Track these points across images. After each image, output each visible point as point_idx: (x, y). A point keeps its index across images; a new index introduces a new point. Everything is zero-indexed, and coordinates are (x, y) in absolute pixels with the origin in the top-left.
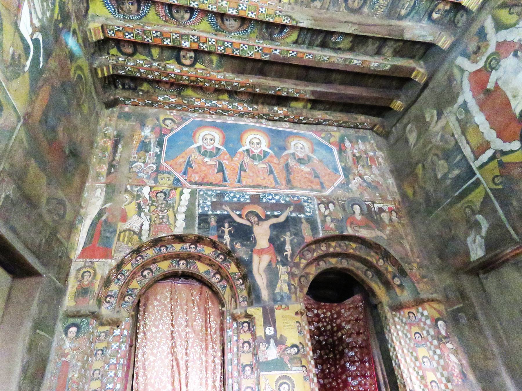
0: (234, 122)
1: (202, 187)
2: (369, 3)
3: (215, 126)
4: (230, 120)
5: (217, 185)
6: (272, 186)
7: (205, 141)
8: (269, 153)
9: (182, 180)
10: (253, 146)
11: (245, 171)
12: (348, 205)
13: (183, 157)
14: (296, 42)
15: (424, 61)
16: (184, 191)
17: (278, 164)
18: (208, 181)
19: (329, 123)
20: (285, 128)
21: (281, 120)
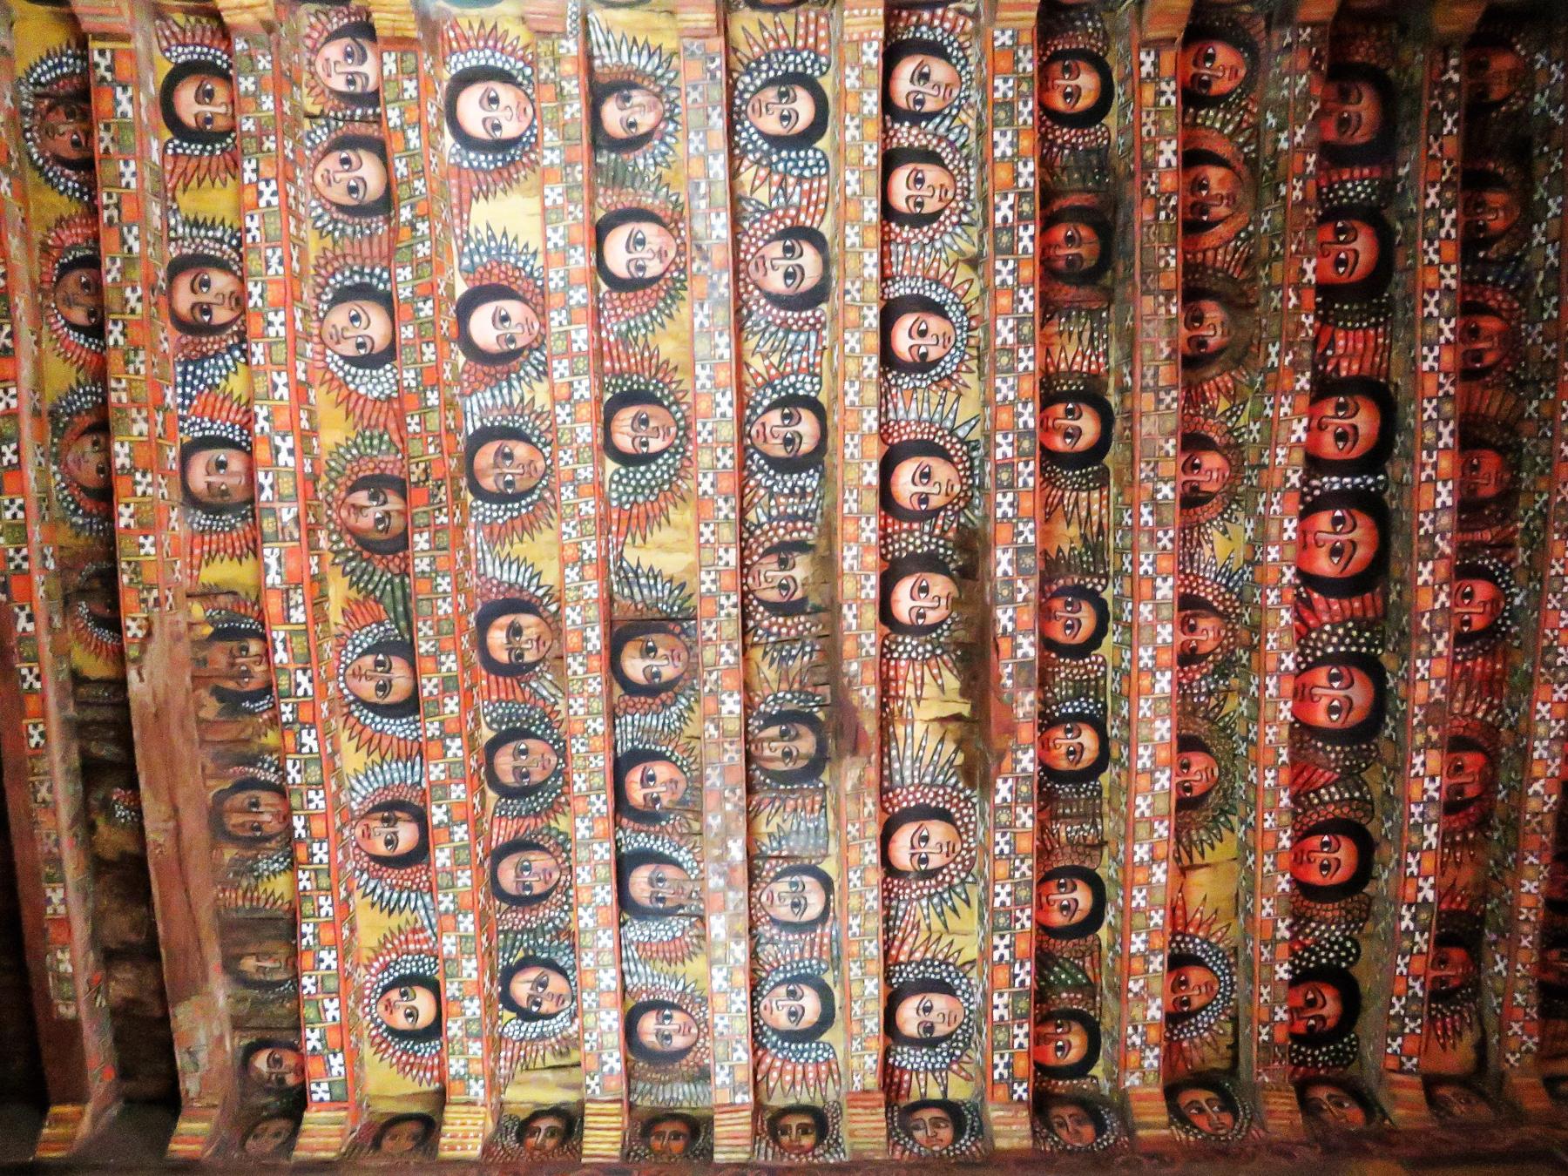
2: (250, 853)
14: (77, 678)
15: (121, 1114)
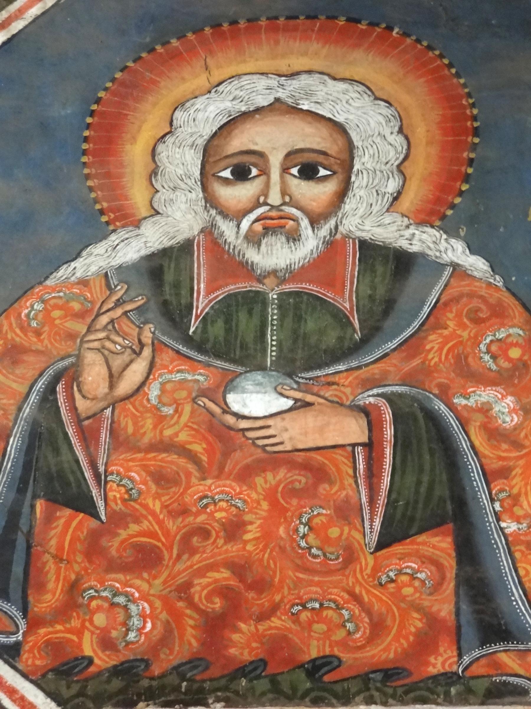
18: (279, 643)
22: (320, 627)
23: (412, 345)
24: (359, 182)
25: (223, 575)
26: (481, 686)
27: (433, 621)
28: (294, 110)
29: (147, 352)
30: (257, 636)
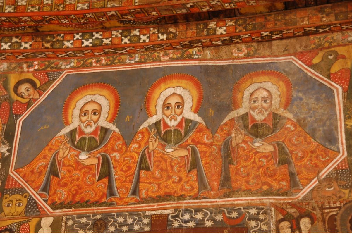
0: (138, 67)
1: (71, 211)
3: (101, 81)
4: (131, 63)
5: (97, 203)
6: (192, 194)
7: (84, 118)
8: (196, 123)
9: (41, 202)
10: (168, 112)
11: (148, 169)
12: (342, 219)
13: (45, 157)
16: (42, 224)
17: (212, 144)
18: (82, 198)
19: (331, 28)
20: (238, 58)
21: (225, 43)
22: (88, 195)
23: (106, 146)
24: (102, 115)
25: (76, 187)
26: (109, 203)
27: (104, 194)
28: (94, 102)
29: (69, 149)
30: (79, 197)
